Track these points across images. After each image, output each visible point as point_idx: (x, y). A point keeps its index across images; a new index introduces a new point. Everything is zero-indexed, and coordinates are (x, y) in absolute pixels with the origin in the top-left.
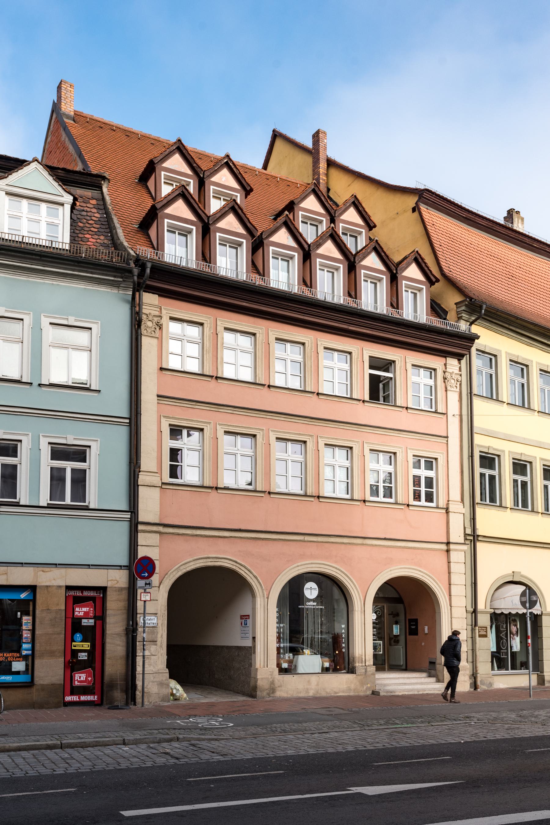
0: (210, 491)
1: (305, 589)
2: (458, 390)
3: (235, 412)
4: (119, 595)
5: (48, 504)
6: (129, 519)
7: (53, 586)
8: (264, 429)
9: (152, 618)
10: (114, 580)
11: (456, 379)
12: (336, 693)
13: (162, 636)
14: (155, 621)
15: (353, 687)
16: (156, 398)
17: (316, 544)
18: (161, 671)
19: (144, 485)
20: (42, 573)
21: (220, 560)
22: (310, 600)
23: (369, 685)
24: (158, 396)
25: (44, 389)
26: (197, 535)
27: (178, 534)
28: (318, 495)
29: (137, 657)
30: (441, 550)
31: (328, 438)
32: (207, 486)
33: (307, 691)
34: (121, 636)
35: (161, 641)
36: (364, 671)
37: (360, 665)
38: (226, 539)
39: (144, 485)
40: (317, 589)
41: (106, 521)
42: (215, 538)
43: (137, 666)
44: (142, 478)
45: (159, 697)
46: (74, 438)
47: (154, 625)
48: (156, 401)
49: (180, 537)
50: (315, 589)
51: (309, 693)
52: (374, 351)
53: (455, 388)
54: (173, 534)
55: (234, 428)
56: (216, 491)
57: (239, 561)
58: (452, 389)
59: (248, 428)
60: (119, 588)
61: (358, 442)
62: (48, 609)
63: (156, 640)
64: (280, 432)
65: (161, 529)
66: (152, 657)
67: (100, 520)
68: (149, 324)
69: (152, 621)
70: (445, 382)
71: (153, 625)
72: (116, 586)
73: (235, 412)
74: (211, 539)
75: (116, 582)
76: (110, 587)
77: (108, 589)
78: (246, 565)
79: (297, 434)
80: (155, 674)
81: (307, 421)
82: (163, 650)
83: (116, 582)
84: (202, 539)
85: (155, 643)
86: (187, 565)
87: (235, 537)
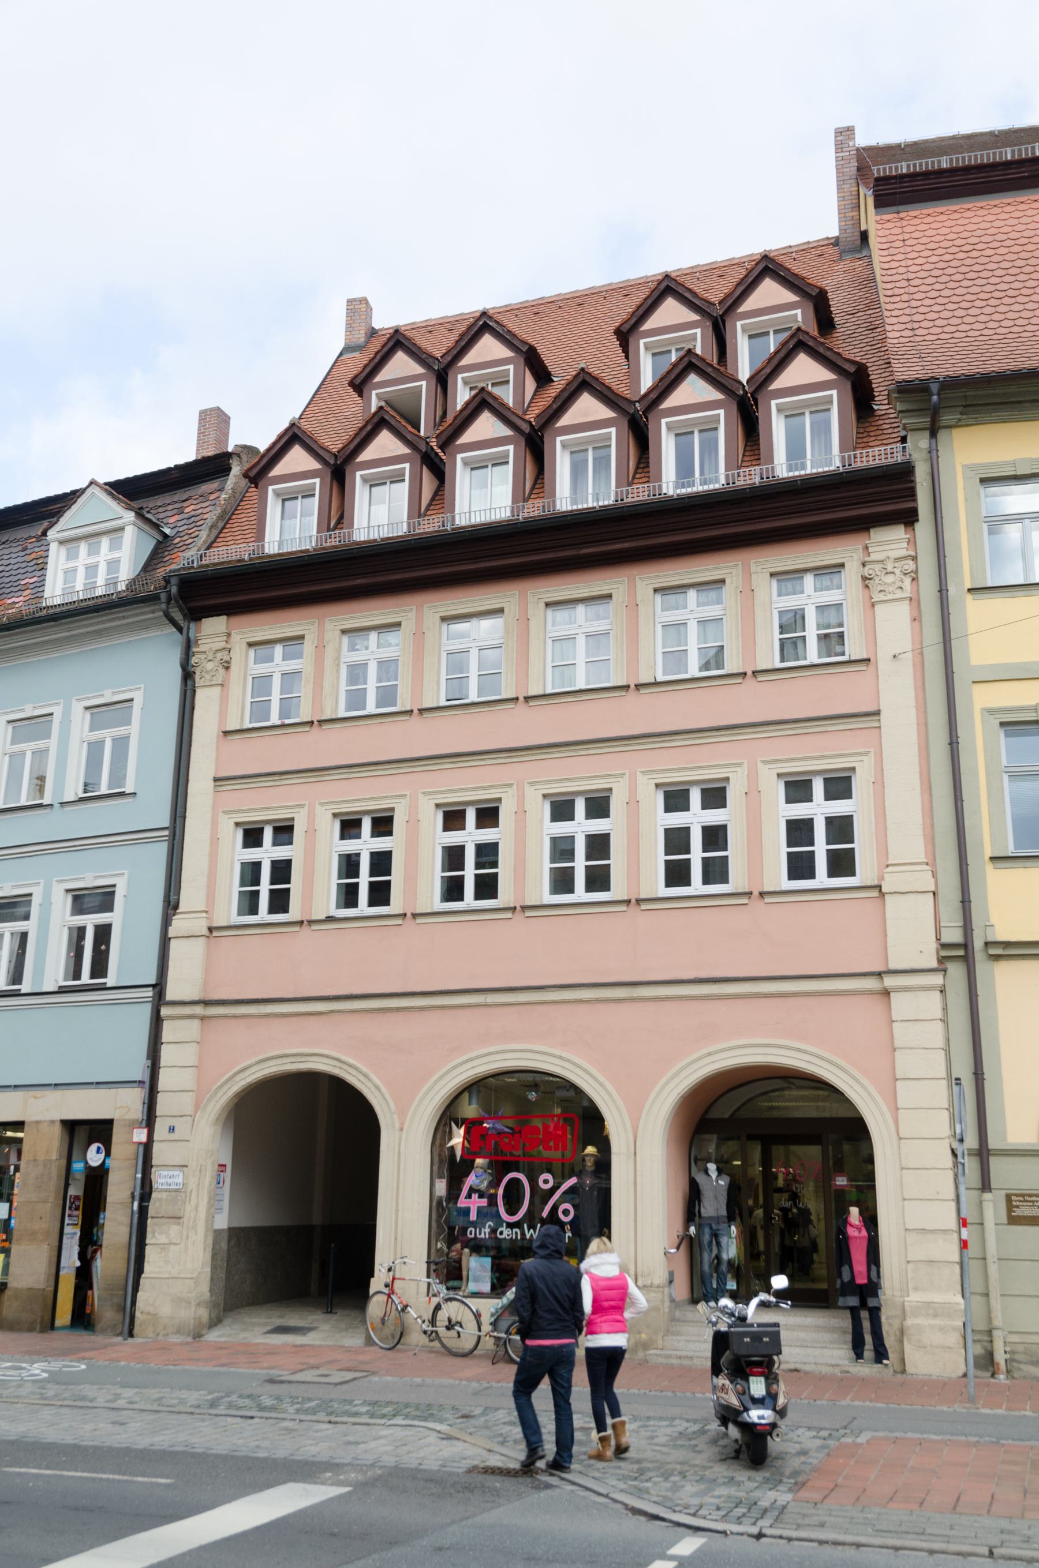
0: (296, 929)
5: (60, 987)
7: (44, 1121)
8: (408, 793)
9: (176, 1173)
11: (897, 571)
14: (180, 1180)
16: (212, 783)
18: (182, 1275)
20: (32, 1099)
24: (216, 780)
25: (67, 809)
27: (235, 1017)
29: (147, 1247)
30: (871, 993)
35: (196, 1216)
42: (302, 1017)
46: (95, 877)
54: (225, 1016)
55: (351, 805)
57: (343, 1058)
61: (623, 775)
62: (35, 1160)
63: (179, 1215)
65: (199, 1010)
66: (172, 1247)
71: (175, 1187)
72: (126, 1117)
74: (294, 1020)
77: (115, 1123)
78: (358, 1065)
79: (478, 788)
80: (170, 1280)
81: (501, 759)
82: (196, 1233)
83: (126, 1110)
85: (178, 1220)
86: (248, 1072)
87: (340, 1011)
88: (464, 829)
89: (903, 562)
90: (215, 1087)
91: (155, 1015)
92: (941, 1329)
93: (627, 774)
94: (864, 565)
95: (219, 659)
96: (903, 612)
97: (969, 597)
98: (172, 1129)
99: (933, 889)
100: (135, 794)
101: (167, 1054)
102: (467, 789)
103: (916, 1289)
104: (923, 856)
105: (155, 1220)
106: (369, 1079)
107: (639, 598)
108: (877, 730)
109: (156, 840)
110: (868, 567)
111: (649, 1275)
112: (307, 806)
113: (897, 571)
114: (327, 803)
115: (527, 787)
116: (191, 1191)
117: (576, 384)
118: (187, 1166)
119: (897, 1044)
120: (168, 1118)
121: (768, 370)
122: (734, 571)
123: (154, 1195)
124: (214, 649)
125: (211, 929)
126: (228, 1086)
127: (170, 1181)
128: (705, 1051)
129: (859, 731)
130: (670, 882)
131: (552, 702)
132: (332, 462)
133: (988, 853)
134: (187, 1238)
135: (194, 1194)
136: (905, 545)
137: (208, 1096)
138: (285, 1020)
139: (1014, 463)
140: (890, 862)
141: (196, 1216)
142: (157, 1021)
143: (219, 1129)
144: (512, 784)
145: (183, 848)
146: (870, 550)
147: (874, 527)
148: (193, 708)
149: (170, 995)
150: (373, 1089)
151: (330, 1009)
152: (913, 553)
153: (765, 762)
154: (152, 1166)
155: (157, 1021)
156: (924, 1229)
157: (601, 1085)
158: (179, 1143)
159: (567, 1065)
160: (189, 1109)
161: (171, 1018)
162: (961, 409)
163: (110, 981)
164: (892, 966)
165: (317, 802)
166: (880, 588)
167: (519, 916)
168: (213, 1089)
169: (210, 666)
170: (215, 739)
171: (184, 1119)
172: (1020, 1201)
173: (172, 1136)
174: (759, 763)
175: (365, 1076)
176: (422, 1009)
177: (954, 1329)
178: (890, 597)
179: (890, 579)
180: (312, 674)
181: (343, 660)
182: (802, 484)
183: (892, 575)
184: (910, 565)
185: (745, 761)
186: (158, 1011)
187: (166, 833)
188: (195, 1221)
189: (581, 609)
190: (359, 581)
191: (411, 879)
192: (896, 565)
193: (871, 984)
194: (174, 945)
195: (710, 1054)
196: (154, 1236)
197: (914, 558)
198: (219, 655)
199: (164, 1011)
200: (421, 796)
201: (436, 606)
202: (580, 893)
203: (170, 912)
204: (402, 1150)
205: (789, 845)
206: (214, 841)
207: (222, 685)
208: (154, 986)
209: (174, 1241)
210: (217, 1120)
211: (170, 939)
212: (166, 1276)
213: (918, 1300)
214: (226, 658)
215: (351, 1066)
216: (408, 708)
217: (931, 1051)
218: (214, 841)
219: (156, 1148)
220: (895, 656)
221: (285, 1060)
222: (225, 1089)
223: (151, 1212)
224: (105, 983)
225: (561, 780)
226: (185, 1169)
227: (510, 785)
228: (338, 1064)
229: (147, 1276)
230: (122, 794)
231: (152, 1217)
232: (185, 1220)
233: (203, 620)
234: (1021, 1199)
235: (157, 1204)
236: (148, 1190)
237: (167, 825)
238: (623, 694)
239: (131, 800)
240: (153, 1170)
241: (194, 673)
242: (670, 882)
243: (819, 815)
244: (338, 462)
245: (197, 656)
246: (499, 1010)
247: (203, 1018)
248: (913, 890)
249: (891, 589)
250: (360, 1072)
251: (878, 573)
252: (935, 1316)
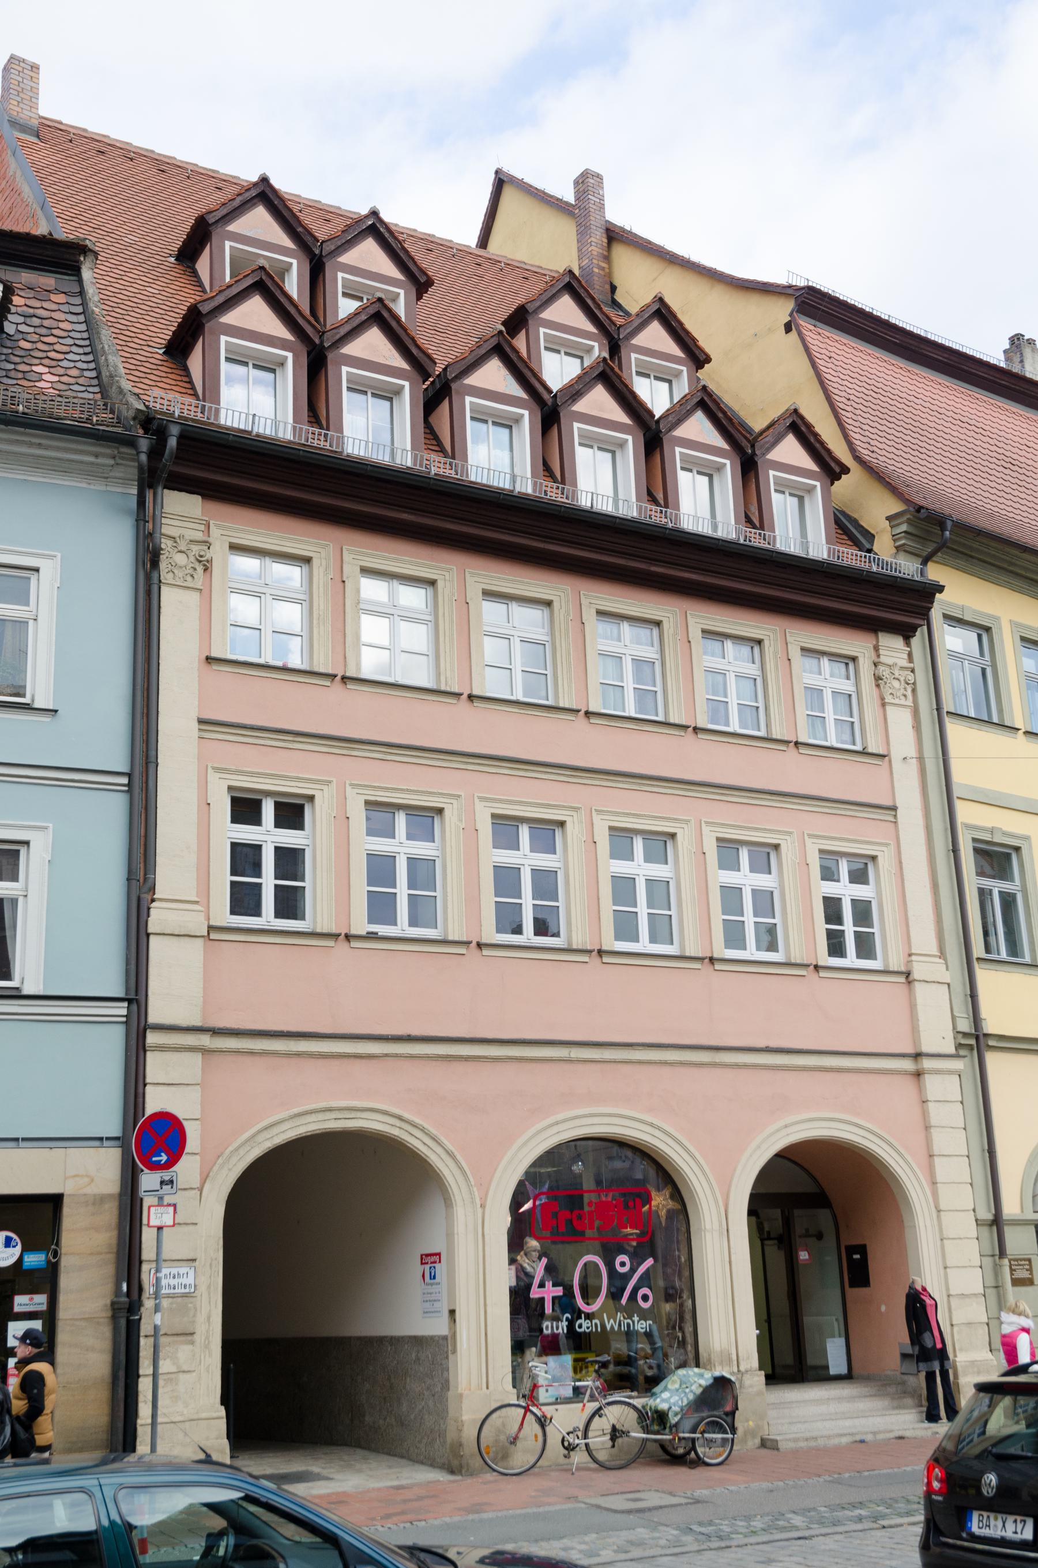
0: (330, 943)
2: (909, 702)
3: (389, 757)
4: (93, 1214)
6: (124, 1019)
9: (182, 1271)
10: (82, 1176)
11: (902, 679)
13: (209, 1318)
14: (190, 1280)
18: (204, 1415)
19: (164, 934)
21: (359, 1114)
26: (299, 1055)
27: (251, 1053)
28: (597, 947)
29: (141, 1380)
32: (325, 931)
34: (98, 1323)
35: (207, 1332)
38: (374, 1062)
39: (164, 934)
42: (346, 1061)
44: (158, 918)
47: (187, 1290)
48: (196, 733)
52: (713, 619)
53: (903, 698)
54: (237, 1052)
56: (346, 944)
57: (406, 1115)
58: (897, 701)
59: (422, 792)
60: (95, 1195)
61: (687, 822)
64: (501, 801)
65: (205, 1040)
66: (182, 1376)
68: (180, 559)
69: (180, 1280)
70: (878, 686)
71: (183, 1291)
73: (389, 757)
74: (335, 1063)
75: (86, 1180)
76: (70, 1195)
77: (66, 1200)
78: (426, 1126)
80: (187, 1424)
81: (563, 776)
82: (210, 1355)
83: (86, 1180)
85: (189, 1338)
86: (275, 1130)
87: (397, 1056)
89: (906, 672)
90: (231, 1148)
94: (875, 665)
102: (530, 803)
112: (334, 784)
114: (361, 785)
119: (933, 1121)
128: (782, 1123)
130: (236, 909)
131: (530, 713)
146: (881, 652)
147: (882, 631)
149: (153, 1018)
151: (385, 1052)
166: (890, 691)
168: (228, 1152)
182: (866, 575)
184: (911, 678)
188: (207, 1338)
189: (625, 626)
190: (405, 516)
193: (908, 1065)
195: (786, 1126)
202: (851, 959)
209: (185, 1368)
213: (966, 1359)
222: (242, 1152)
225: (628, 814)
228: (398, 1123)
231: (146, 1336)
232: (196, 1337)
237: (124, 768)
239: (48, 720)
242: (236, 909)
243: (402, 854)
246: (581, 1067)
247: (205, 1051)
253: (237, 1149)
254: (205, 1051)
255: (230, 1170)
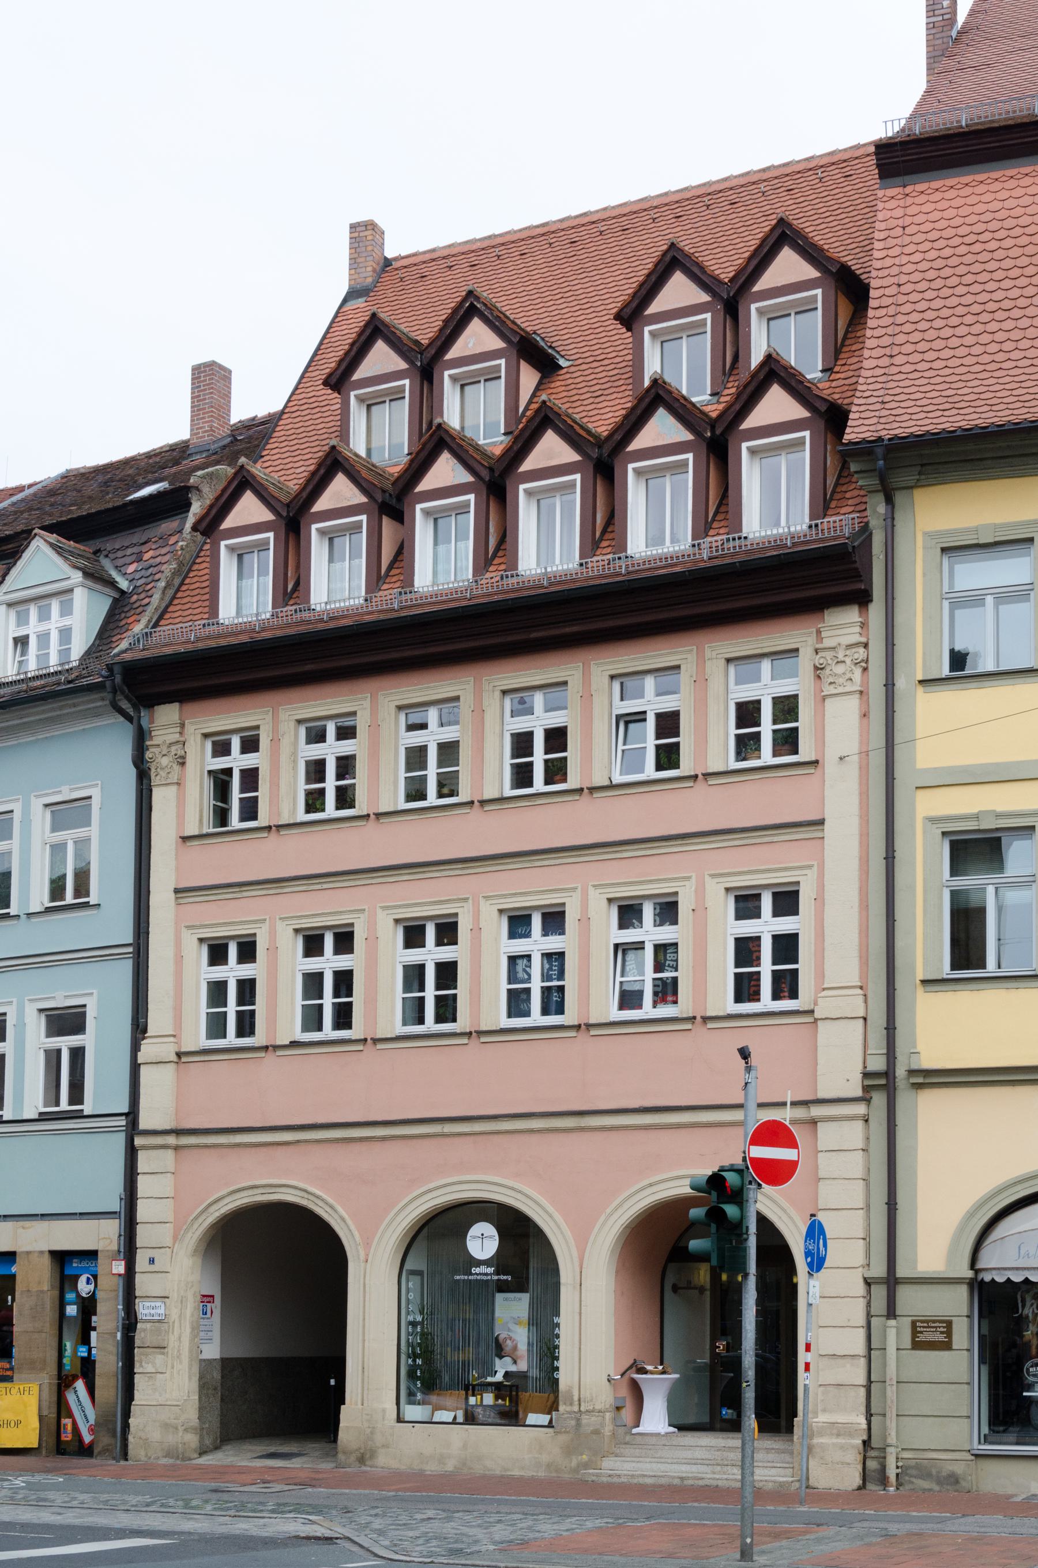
1: (468, 1238)
5: (41, 1114)
6: (124, 1128)
7: (34, 1252)
8: (366, 907)
9: (158, 1304)
11: (848, 660)
12: (506, 1470)
13: (180, 1338)
14: (162, 1311)
15: (545, 1458)
16: (173, 895)
17: (472, 1138)
18: (169, 1403)
20: (21, 1230)
22: (480, 1263)
23: (584, 1457)
24: (177, 891)
25: (34, 920)
31: (504, 896)
33: (442, 1459)
35: (179, 1346)
36: (573, 1423)
37: (568, 1409)
38: (292, 1147)
40: (497, 1237)
41: (97, 1135)
43: (135, 1392)
45: (163, 1450)
46: (65, 996)
49: (212, 1151)
50: (491, 1237)
51: (444, 1464)
54: (197, 1146)
59: (335, 913)
61: (574, 889)
62: (29, 1291)
64: (400, 907)
65: (171, 1140)
66: (158, 1375)
67: (110, 1134)
74: (264, 1150)
76: (101, 1251)
77: (99, 1254)
78: (325, 1196)
82: (181, 1363)
83: (109, 1241)
84: (248, 1150)
85: (162, 1350)
87: (306, 1141)
88: (424, 946)
90: (191, 1218)
91: (129, 1146)
92: (842, 1447)
93: (579, 889)
94: (817, 651)
95: (173, 753)
96: (853, 704)
97: (920, 689)
98: (152, 1261)
99: (862, 1014)
100: (99, 905)
101: (144, 1185)
102: (423, 903)
103: (824, 1410)
104: (857, 979)
105: (141, 1350)
106: (336, 1211)
107: (594, 687)
108: (820, 841)
109: (121, 957)
110: (820, 654)
111: (591, 1400)
113: (848, 660)
115: (482, 901)
116: (174, 1322)
117: (538, 420)
118: (168, 1298)
120: (148, 1250)
121: (737, 407)
122: (689, 656)
123: (139, 1326)
124: (168, 742)
125: (179, 1055)
126: (203, 1217)
127: (152, 1312)
129: (804, 842)
132: (285, 514)
133: (920, 976)
134: (173, 1368)
135: (177, 1324)
136: (858, 629)
137: (185, 1227)
138: (253, 1150)
139: (976, 530)
140: (826, 986)
141: (179, 1346)
142: (131, 1153)
143: (199, 1261)
144: (468, 899)
145: (148, 967)
146: (823, 634)
147: (828, 608)
148: (151, 810)
149: (144, 1124)
150: (339, 1221)
152: (863, 640)
153: (712, 876)
154: (136, 1297)
155: (131, 1153)
156: (834, 1355)
157: (551, 1216)
158: (160, 1275)
159: (519, 1196)
160: (168, 1242)
161: (145, 1148)
162: (919, 468)
163: (87, 1108)
164: (822, 1094)
165: (278, 917)
166: (831, 680)
167: (474, 1041)
168: (189, 1221)
169: (165, 761)
170: (174, 846)
171: (163, 1250)
172: (924, 1327)
173: (152, 1268)
174: (707, 877)
175: (331, 1207)
176: (384, 1139)
177: (853, 1447)
178: (840, 690)
179: (839, 669)
180: (268, 772)
181: (301, 754)
183: (843, 664)
185: (694, 875)
186: (132, 1140)
187: (130, 950)
188: (179, 1351)
191: (371, 1001)
192: (848, 652)
194: (144, 1071)
195: (651, 1185)
196: (141, 1366)
197: (866, 646)
198: (173, 749)
199: (138, 1141)
200: (379, 911)
201: (391, 693)
203: (140, 1036)
204: (367, 1282)
205: (737, 966)
206: (179, 959)
207: (178, 784)
208: (126, 1115)
210: (195, 1251)
211: (140, 1064)
212: (155, 1403)
214: (181, 753)
215: (318, 1197)
216: (365, 813)
217: (850, 1181)
218: (179, 959)
219: (139, 1279)
220: (841, 759)
221: (256, 1191)
222: (200, 1220)
223: (138, 1342)
224: (82, 1110)
225: (515, 894)
226: (166, 1300)
227: (466, 900)
228: (306, 1195)
229: (138, 1403)
230: (86, 905)
232: (169, 1350)
233: (156, 708)
234: (926, 1325)
235: (143, 1335)
236: (133, 1321)
237: (131, 941)
238: (577, 797)
240: (137, 1301)
241: (149, 769)
244: (291, 514)
245: (152, 750)
246: (457, 1140)
247: (177, 1148)
248: (843, 1016)
249: (841, 680)
250: (326, 1203)
251: (830, 662)
252: (838, 1435)
253: (196, 1218)
254: (177, 1148)
255: (193, 1233)
